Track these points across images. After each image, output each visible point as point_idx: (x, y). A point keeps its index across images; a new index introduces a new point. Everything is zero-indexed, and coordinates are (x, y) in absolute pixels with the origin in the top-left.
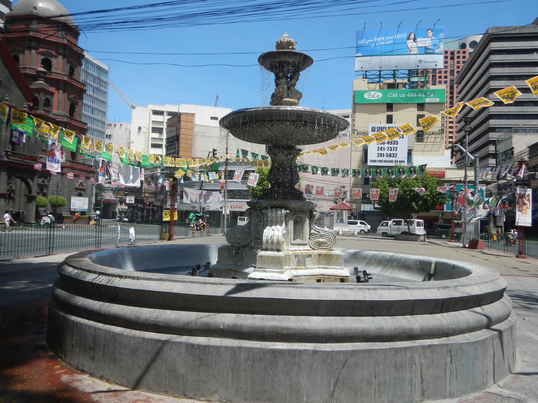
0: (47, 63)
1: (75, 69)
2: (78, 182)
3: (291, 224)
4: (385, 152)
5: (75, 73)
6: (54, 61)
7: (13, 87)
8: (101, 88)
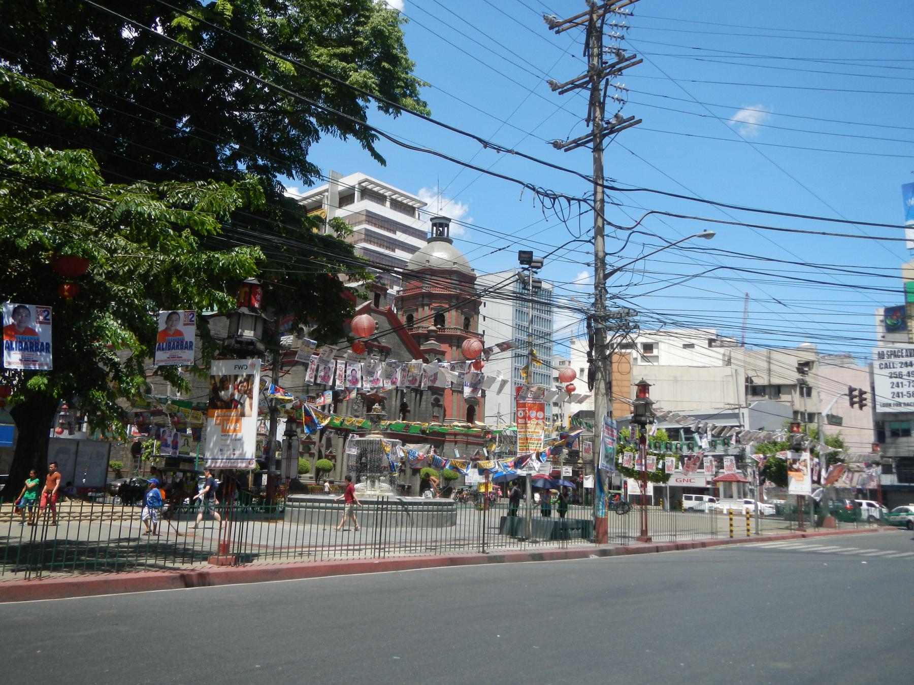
0: (439, 319)
1: (471, 320)
2: (474, 451)
3: (369, 482)
4: (905, 390)
5: (471, 323)
6: (447, 315)
7: (402, 352)
8: (543, 315)
